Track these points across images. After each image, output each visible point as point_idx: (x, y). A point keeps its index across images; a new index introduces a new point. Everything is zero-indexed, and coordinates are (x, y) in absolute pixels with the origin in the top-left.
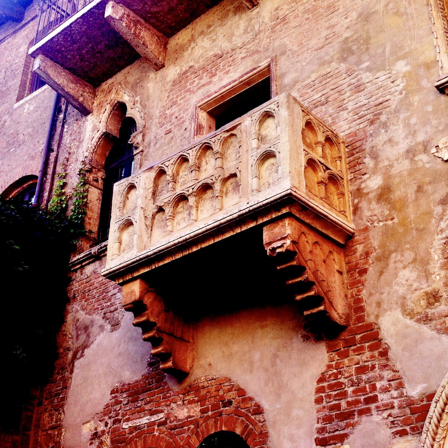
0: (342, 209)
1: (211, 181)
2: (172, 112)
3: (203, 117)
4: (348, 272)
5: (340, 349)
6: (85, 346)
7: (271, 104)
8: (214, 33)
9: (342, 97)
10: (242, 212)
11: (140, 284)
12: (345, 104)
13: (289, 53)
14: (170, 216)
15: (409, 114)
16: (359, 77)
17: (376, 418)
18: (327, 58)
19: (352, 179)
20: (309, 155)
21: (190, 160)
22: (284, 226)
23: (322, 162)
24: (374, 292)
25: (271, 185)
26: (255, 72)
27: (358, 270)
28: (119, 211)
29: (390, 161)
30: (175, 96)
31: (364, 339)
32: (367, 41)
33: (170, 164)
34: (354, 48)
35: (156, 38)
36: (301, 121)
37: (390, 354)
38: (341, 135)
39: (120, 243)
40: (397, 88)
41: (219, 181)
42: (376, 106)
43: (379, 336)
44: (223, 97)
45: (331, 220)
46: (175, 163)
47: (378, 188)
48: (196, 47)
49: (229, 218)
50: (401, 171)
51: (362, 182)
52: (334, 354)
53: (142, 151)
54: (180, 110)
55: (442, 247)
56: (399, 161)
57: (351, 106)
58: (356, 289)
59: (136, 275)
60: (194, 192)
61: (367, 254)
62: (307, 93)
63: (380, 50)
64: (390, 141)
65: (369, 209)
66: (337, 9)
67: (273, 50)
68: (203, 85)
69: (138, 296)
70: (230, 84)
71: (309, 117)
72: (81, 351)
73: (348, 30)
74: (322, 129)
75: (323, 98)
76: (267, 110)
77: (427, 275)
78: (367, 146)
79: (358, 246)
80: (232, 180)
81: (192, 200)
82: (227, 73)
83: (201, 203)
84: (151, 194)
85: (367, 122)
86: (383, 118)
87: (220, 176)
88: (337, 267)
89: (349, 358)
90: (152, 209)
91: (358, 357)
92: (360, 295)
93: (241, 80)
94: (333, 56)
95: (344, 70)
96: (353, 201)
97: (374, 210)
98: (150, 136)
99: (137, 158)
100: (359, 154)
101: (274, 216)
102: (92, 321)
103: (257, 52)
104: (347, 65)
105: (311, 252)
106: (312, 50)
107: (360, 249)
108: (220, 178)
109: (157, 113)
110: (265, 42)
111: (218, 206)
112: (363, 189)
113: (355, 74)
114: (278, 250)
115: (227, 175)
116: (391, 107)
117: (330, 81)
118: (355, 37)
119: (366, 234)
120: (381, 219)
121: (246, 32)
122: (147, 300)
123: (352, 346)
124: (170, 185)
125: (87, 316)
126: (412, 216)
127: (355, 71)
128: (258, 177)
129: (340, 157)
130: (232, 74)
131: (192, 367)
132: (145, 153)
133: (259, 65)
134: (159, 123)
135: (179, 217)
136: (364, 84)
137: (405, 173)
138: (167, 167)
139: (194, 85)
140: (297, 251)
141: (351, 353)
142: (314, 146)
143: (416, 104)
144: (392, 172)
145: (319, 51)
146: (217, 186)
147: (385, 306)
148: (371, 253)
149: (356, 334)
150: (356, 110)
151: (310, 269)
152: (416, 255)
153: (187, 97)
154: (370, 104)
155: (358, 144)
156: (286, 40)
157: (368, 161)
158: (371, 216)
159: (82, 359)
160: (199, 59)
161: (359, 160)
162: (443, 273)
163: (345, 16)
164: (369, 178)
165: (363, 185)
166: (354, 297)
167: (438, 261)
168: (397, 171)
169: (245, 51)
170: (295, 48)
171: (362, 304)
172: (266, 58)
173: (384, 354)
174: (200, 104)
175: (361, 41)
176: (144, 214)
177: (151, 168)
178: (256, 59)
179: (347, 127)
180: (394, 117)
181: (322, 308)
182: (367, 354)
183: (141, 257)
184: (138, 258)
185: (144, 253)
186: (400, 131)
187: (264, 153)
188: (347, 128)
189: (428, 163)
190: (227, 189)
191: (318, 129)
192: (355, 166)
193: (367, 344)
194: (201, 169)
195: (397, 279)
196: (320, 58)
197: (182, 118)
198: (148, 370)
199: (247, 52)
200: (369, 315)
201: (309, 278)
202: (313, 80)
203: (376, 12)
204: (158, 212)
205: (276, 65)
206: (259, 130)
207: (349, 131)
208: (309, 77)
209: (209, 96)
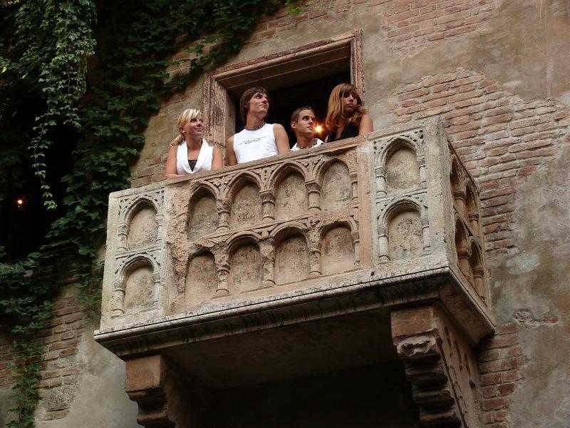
1: (304, 227)
10: (364, 285)
12: (479, 135)
13: (385, 33)
14: (225, 266)
16: (503, 99)
18: (450, 57)
19: (492, 250)
21: (262, 186)
22: (429, 317)
24: (522, 419)
25: (408, 253)
27: (499, 385)
28: (122, 239)
33: (222, 183)
34: (496, 53)
39: (124, 292)
40: (564, 131)
41: (317, 230)
42: (530, 149)
45: (477, 311)
46: (232, 185)
47: (533, 271)
49: (340, 290)
51: (507, 258)
57: (489, 140)
58: (495, 413)
60: (271, 237)
61: (514, 365)
63: (537, 68)
64: (552, 205)
65: (519, 300)
67: (355, 21)
69: (158, 381)
73: (485, 23)
76: (403, 137)
79: (499, 350)
80: (340, 231)
81: (266, 249)
83: (281, 256)
84: (184, 224)
86: (541, 169)
87: (319, 221)
90: (187, 247)
93: (297, 54)
94: (459, 57)
95: (478, 84)
96: (493, 284)
103: (325, 15)
104: (484, 76)
107: (501, 355)
112: (509, 268)
114: (416, 350)
118: (495, 37)
119: (512, 335)
120: (537, 318)
122: (168, 389)
124: (223, 217)
127: (496, 89)
130: (278, 40)
133: (333, 39)
135: (238, 270)
136: (511, 112)
138: (218, 187)
145: (436, 42)
146: (314, 236)
154: (521, 144)
155: (501, 200)
156: (379, 11)
157: (518, 230)
158: (521, 310)
161: (503, 225)
165: (509, 263)
166: (492, 423)
170: (395, 28)
172: (344, 30)
175: (507, 46)
176: (172, 253)
177: (185, 183)
178: (324, 27)
180: (558, 172)
183: (175, 322)
184: (167, 323)
185: (180, 317)
187: (398, 202)
188: (483, 172)
190: (328, 243)
194: (278, 201)
195: (561, 407)
204: (195, 255)
205: (361, 47)
207: (486, 177)
208: (419, 79)
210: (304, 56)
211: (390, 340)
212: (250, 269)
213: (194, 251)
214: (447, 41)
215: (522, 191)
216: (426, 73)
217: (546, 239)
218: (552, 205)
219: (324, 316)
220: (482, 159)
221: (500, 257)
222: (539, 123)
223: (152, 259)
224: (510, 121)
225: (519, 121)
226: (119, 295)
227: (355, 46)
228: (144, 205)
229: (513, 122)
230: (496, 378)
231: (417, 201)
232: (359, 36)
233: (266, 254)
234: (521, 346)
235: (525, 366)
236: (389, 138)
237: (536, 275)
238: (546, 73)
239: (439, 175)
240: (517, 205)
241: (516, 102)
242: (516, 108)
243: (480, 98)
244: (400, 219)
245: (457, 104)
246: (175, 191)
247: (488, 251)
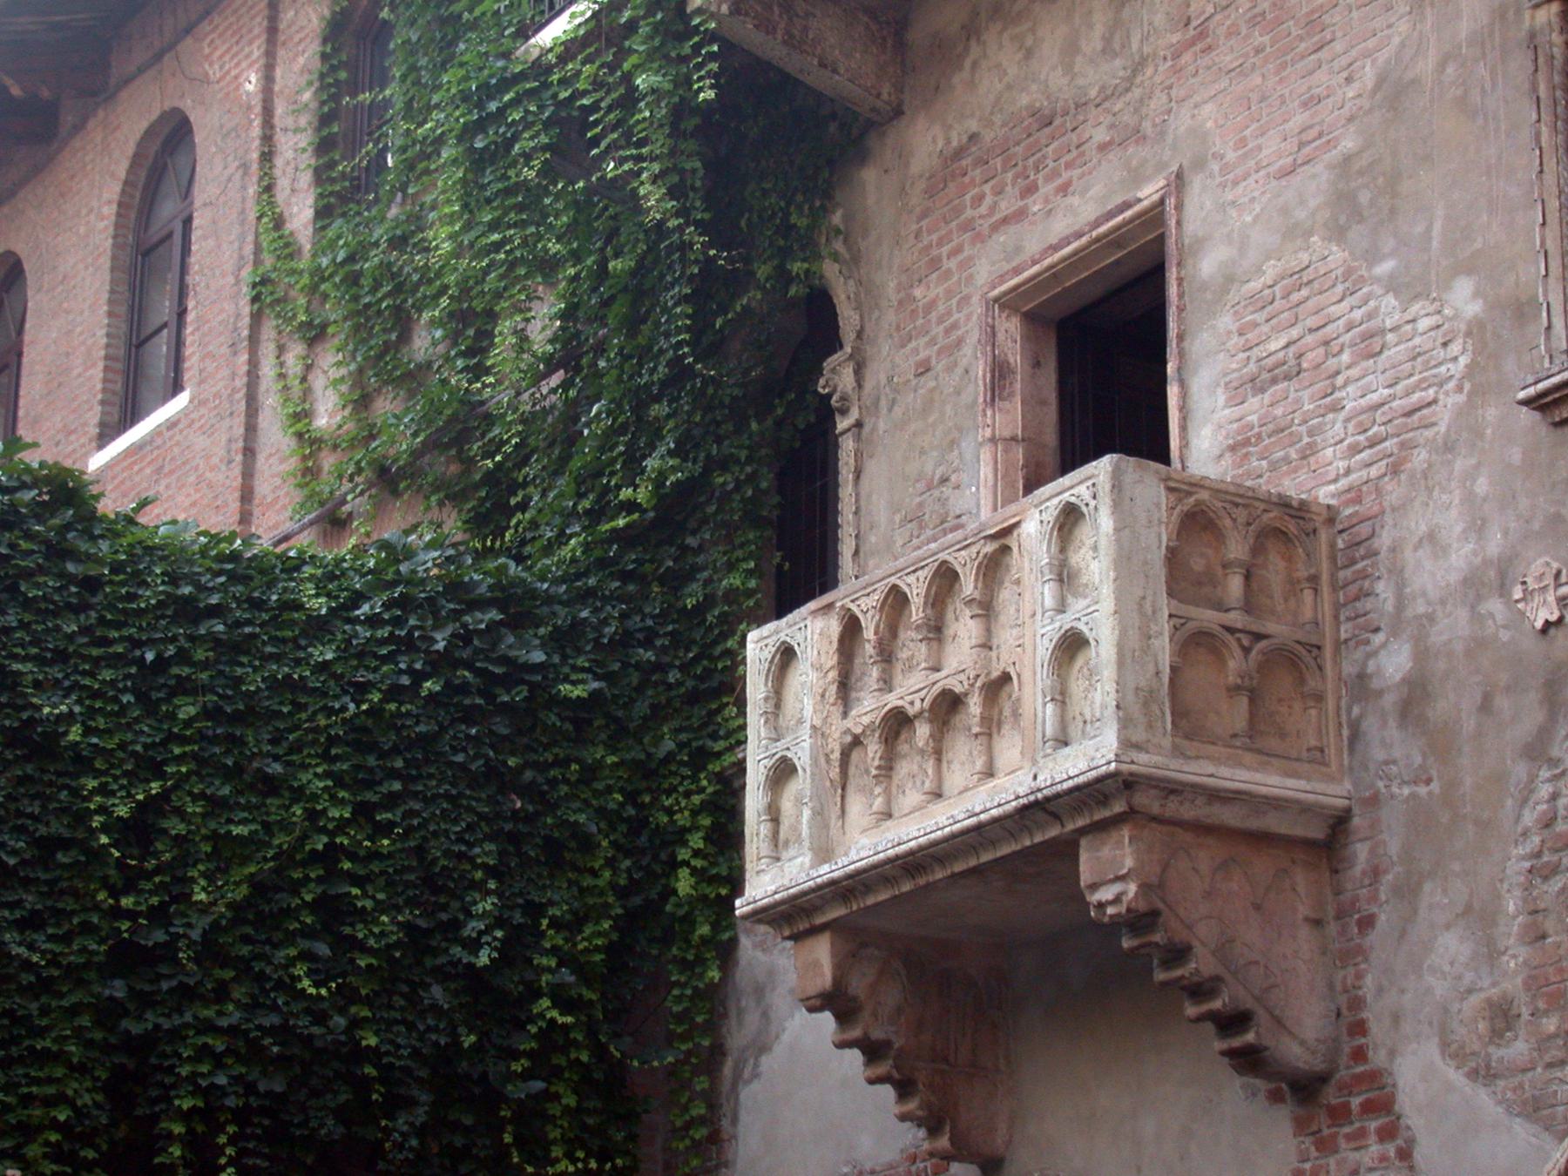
0: (1313, 743)
2: (932, 295)
3: (1010, 328)
4: (1338, 917)
5: (1320, 1131)
6: (764, 1049)
7: (1081, 482)
8: (1030, 24)
9: (1332, 363)
10: (1022, 801)
11: (832, 944)
14: (879, 768)
15: (1473, 461)
16: (1372, 303)
18: (1301, 214)
20: (1190, 625)
22: (1123, 848)
23: (1239, 626)
26: (1128, 214)
29: (1429, 603)
30: (935, 237)
31: (1369, 1108)
34: (1364, 198)
35: (866, 19)
36: (1163, 528)
37: (1418, 1155)
38: (1325, 495)
41: (977, 691)
43: (1396, 1107)
44: (1055, 274)
47: (1403, 680)
48: (984, 64)
49: (995, 812)
50: (1450, 641)
51: (1369, 656)
52: (1308, 1140)
53: (859, 425)
54: (949, 294)
55: (1522, 879)
56: (1449, 608)
59: (819, 920)
61: (1376, 873)
62: (1256, 325)
63: (1419, 229)
64: (1431, 537)
65: (1384, 744)
66: (1329, 37)
68: (1005, 221)
70: (1066, 241)
71: (1192, 500)
72: (752, 1061)
74: (1241, 515)
75: (1292, 349)
76: (1073, 499)
77: (1491, 954)
79: (1359, 845)
81: (923, 731)
82: (1064, 190)
83: (948, 737)
84: (834, 688)
85: (1384, 462)
86: (1420, 458)
88: (1303, 910)
89: (1338, 1156)
91: (1357, 1155)
92: (1360, 988)
93: (1094, 234)
94: (1313, 214)
95: (1339, 272)
97: (1391, 746)
98: (876, 375)
99: (847, 446)
100: (1365, 563)
101: (1097, 817)
102: (771, 973)
103: (1136, 135)
105: (1208, 895)
106: (1268, 175)
108: (978, 684)
109: (891, 288)
110: (1158, 101)
111: (980, 764)
112: (1370, 677)
113: (1365, 290)
114: (1110, 910)
115: (995, 674)
116: (1436, 429)
117: (1308, 298)
118: (1363, 162)
121: (1108, 51)
122: (858, 985)
123: (1341, 1126)
125: (759, 954)
126: (1468, 781)
127: (1362, 279)
128: (1061, 697)
129: (1314, 580)
130: (1075, 200)
131: (1010, 1141)
132: (866, 429)
133: (1140, 195)
134: (898, 328)
135: (904, 768)
136: (1382, 332)
137: (1459, 647)
139: (983, 209)
140: (1161, 905)
141: (1342, 1143)
142: (1220, 571)
143: (1489, 431)
144: (1433, 639)
145: (1284, 182)
146: (974, 706)
147: (1407, 1027)
148: (1386, 872)
149: (1350, 1094)
150: (1364, 417)
151: (1202, 943)
152: (1471, 895)
153: (966, 254)
154: (1395, 404)
155: (1364, 530)
158: (1387, 763)
159: (755, 1086)
160: (992, 113)
161: (1367, 583)
162: (1523, 952)
163: (1345, 74)
164: (1384, 645)
165: (1371, 666)
167: (1515, 917)
168: (1444, 638)
169: (1109, 119)
170: (1231, 156)
171: (1364, 1015)
173: (1405, 1154)
174: (996, 292)
175: (1381, 180)
177: (830, 606)
179: (1342, 465)
181: (1250, 1037)
182: (1375, 1149)
183: (819, 880)
185: (826, 872)
186: (1454, 513)
189: (1505, 627)
190: (1001, 713)
191: (1228, 522)
192: (1357, 599)
193: (1373, 1125)
196: (1285, 211)
197: (955, 326)
198: (915, 1137)
199: (1112, 126)
200: (1376, 1048)
201: (1201, 968)
202: (1270, 282)
203: (1414, 81)
205: (1179, 207)
206: (1063, 550)
208: (1259, 271)
209: (1017, 271)
210: (1105, 235)
211: (1077, 898)
212: (915, 767)
213: (849, 739)
214: (1296, 180)
215: (1393, 510)
216: (1268, 258)
217: (1421, 609)
218: (1431, 537)
219: (999, 854)
220: (1341, 441)
221: (1358, 654)
222: (1419, 354)
223: (796, 761)
224: (1381, 352)
225: (1393, 350)
226: (765, 829)
227: (1171, 203)
228: (787, 655)
229: (1386, 353)
230: (1353, 904)
231: (1085, 629)
232: (1179, 181)
233: (921, 744)
234: (1385, 836)
235: (1390, 877)
236: (1055, 501)
237: (1406, 690)
238: (1431, 238)
239: (1112, 574)
240: (1384, 540)
242: (1389, 324)
243: (1344, 304)
244: (1080, 662)
245: (1311, 322)
246: (818, 624)
247: (1346, 641)
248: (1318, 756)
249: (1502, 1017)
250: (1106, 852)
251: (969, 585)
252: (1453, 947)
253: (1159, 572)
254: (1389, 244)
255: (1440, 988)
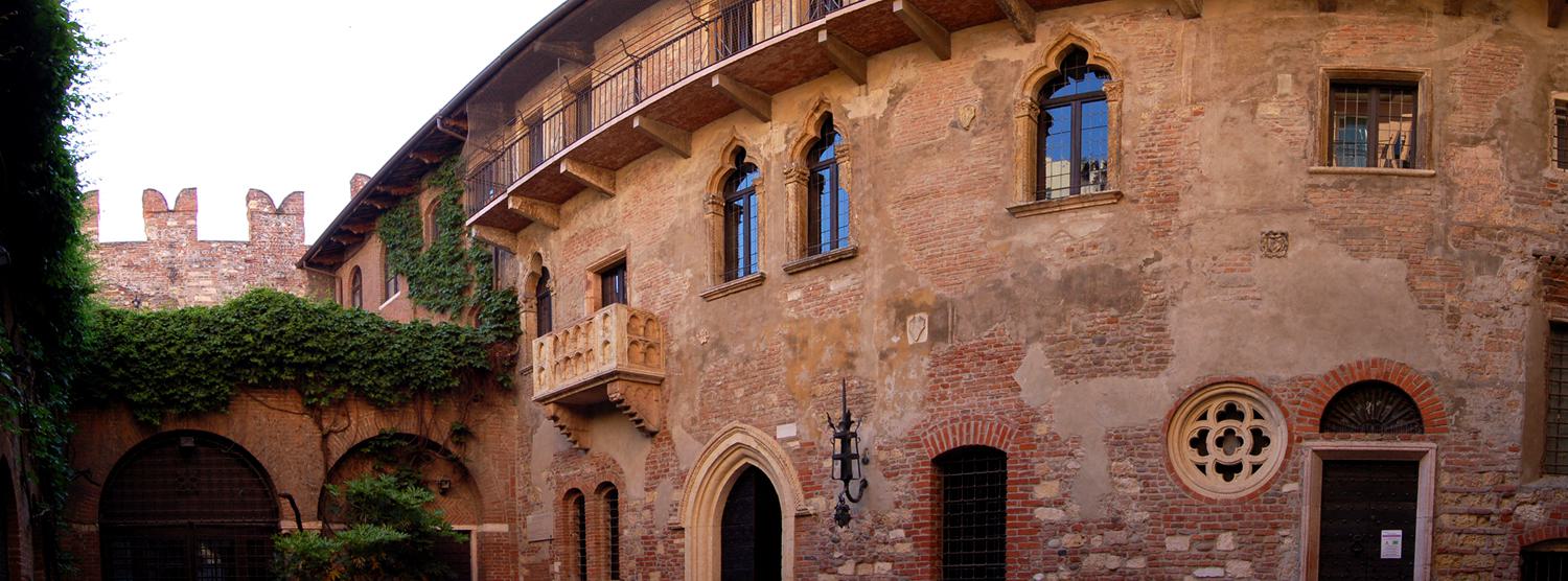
17: (668, 480)
31: (666, 438)
32: (673, 248)
38: (656, 313)
57: (662, 293)
61: (670, 391)
64: (679, 323)
78: (669, 323)
88: (654, 398)
146: (584, 356)
173: (673, 448)
181: (642, 424)
203: (679, 228)
218: (679, 323)
232: (629, 246)
241: (672, 274)
248: (659, 367)
249: (694, 420)
250: (613, 387)
251: (583, 330)
252: (685, 406)
253: (626, 328)
254: (672, 259)
255: (682, 415)
